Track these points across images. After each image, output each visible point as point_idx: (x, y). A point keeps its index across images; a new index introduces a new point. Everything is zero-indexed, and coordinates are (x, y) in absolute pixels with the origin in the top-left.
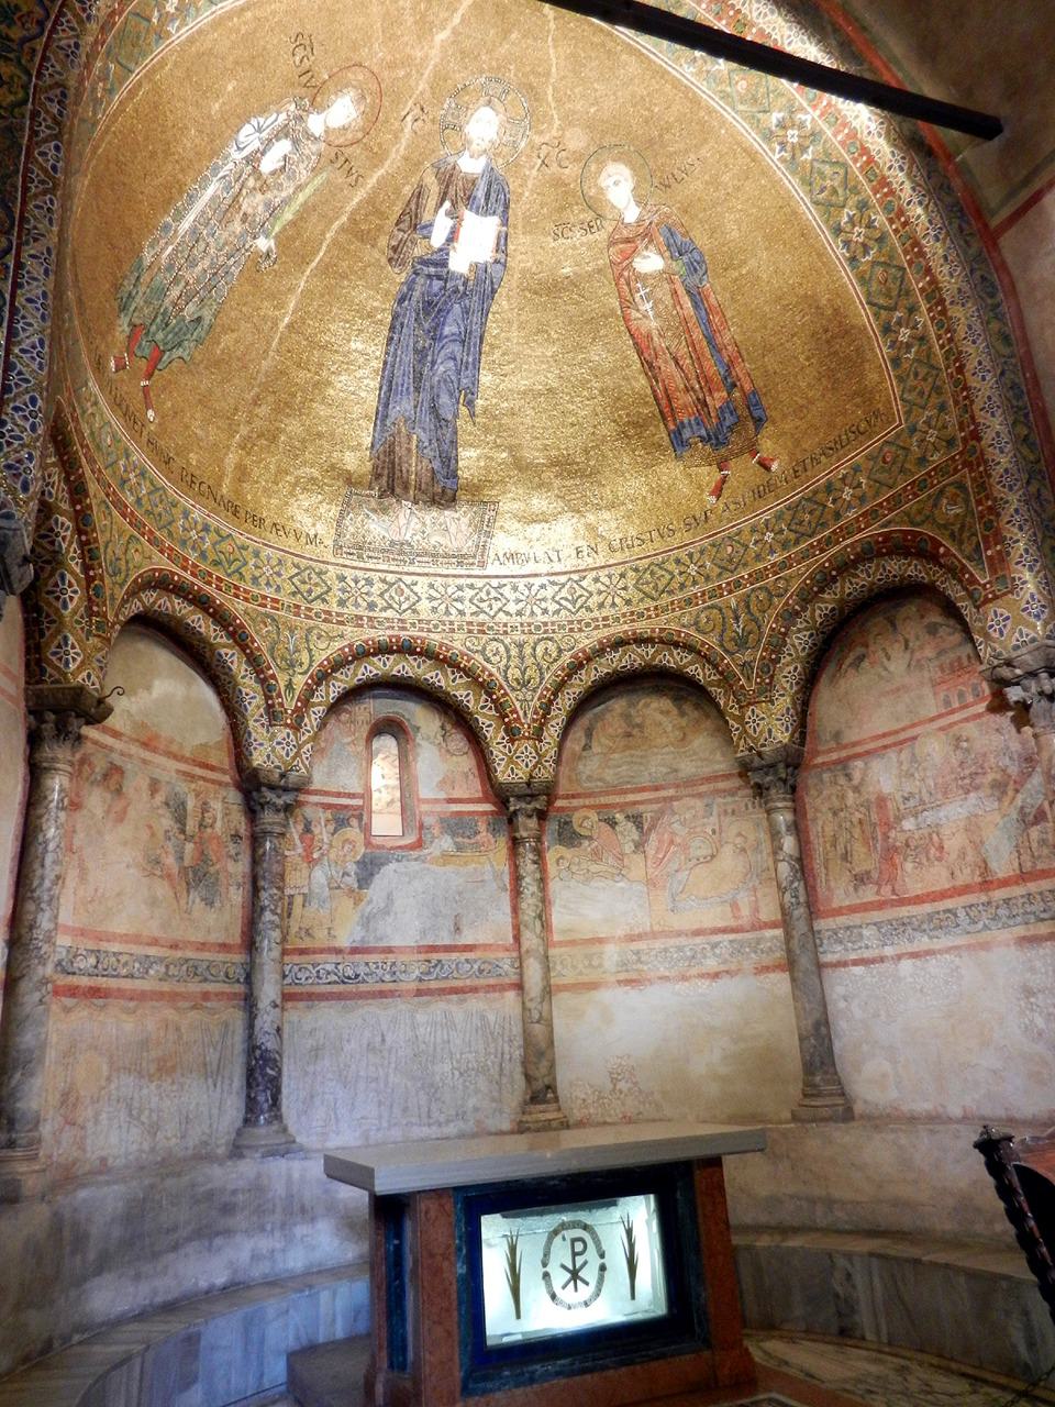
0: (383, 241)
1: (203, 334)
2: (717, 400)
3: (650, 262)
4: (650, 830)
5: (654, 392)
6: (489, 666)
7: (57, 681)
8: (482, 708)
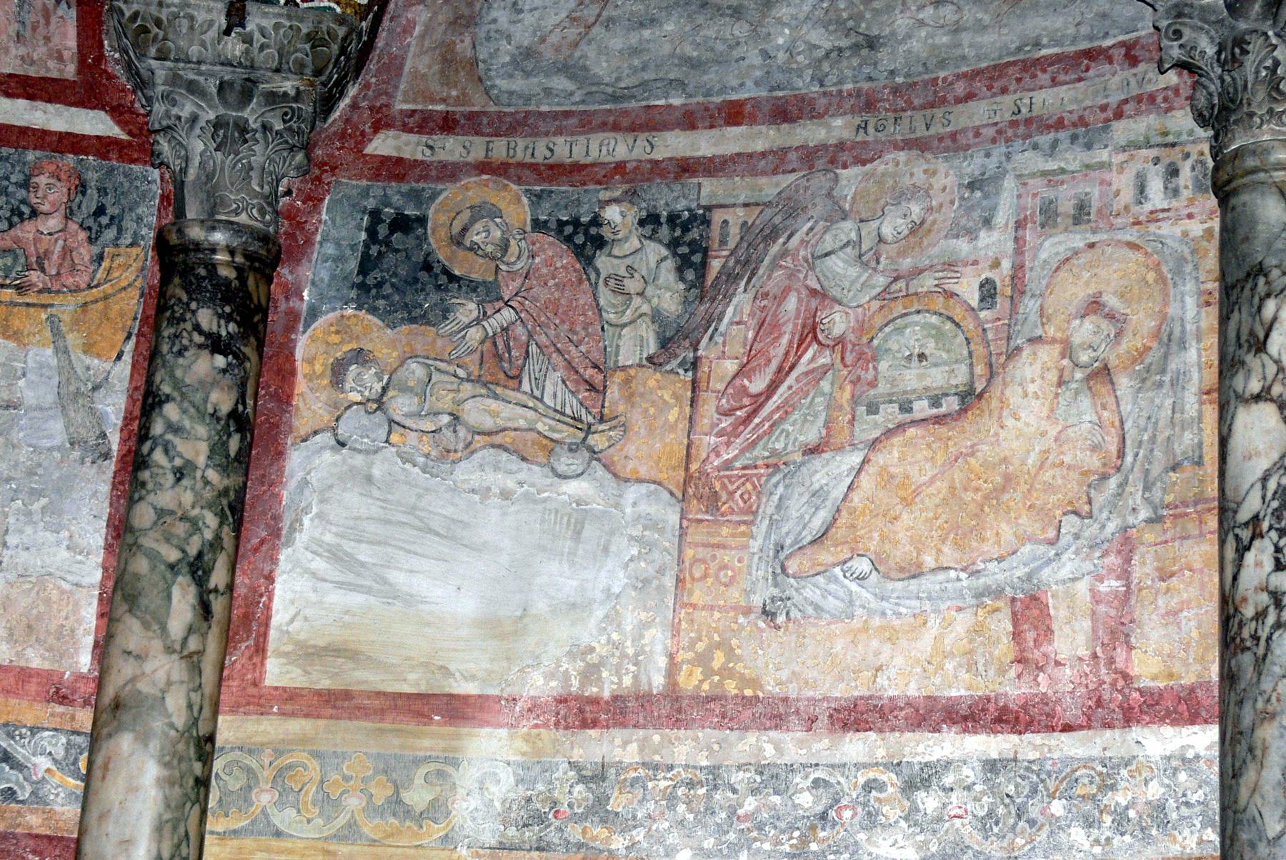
4: (730, 277)
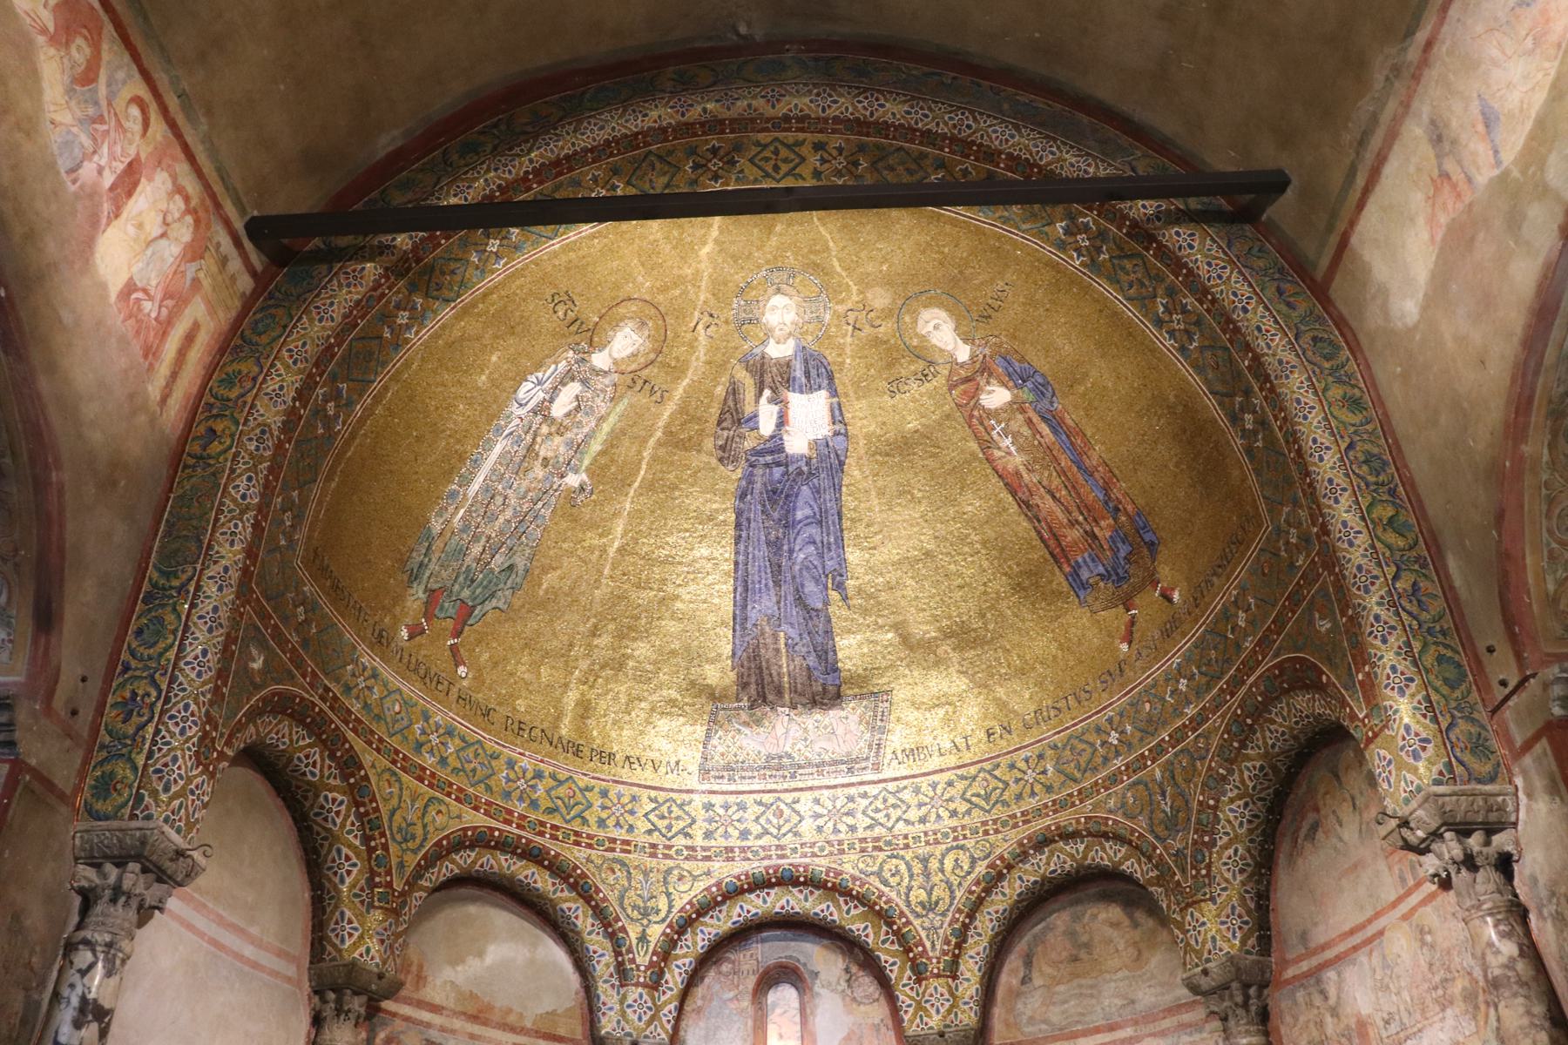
0: (709, 444)
1: (518, 580)
2: (1104, 530)
3: (996, 396)
5: (1039, 533)
6: (886, 890)
7: (334, 959)
8: (884, 942)
